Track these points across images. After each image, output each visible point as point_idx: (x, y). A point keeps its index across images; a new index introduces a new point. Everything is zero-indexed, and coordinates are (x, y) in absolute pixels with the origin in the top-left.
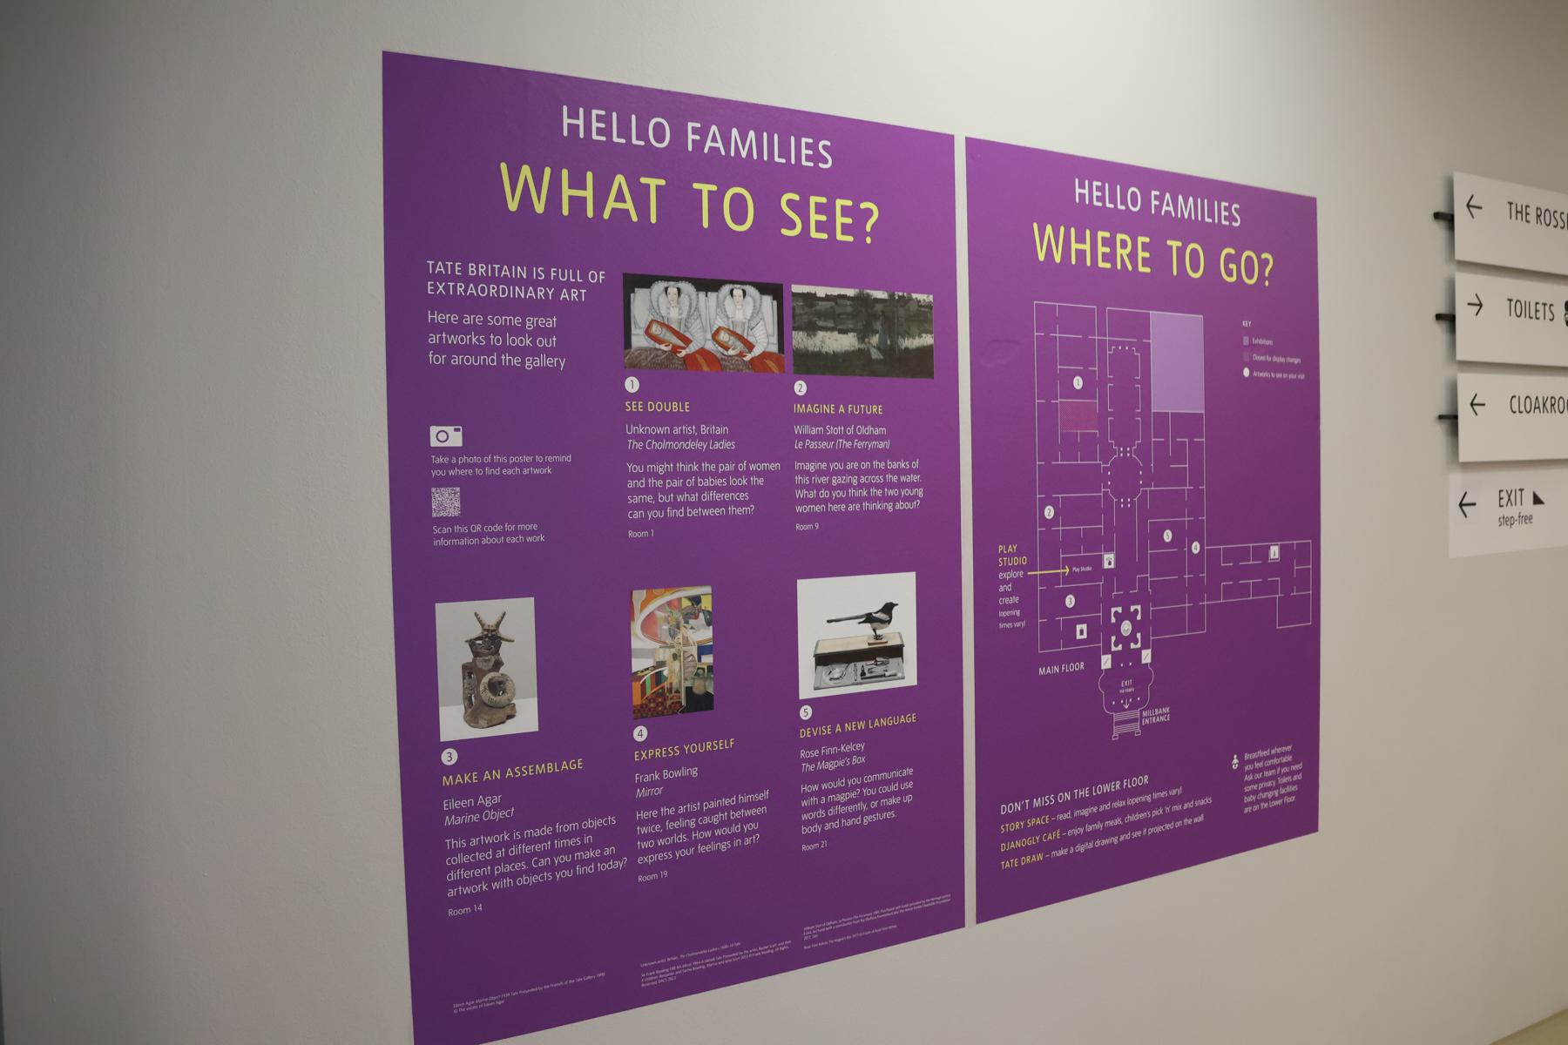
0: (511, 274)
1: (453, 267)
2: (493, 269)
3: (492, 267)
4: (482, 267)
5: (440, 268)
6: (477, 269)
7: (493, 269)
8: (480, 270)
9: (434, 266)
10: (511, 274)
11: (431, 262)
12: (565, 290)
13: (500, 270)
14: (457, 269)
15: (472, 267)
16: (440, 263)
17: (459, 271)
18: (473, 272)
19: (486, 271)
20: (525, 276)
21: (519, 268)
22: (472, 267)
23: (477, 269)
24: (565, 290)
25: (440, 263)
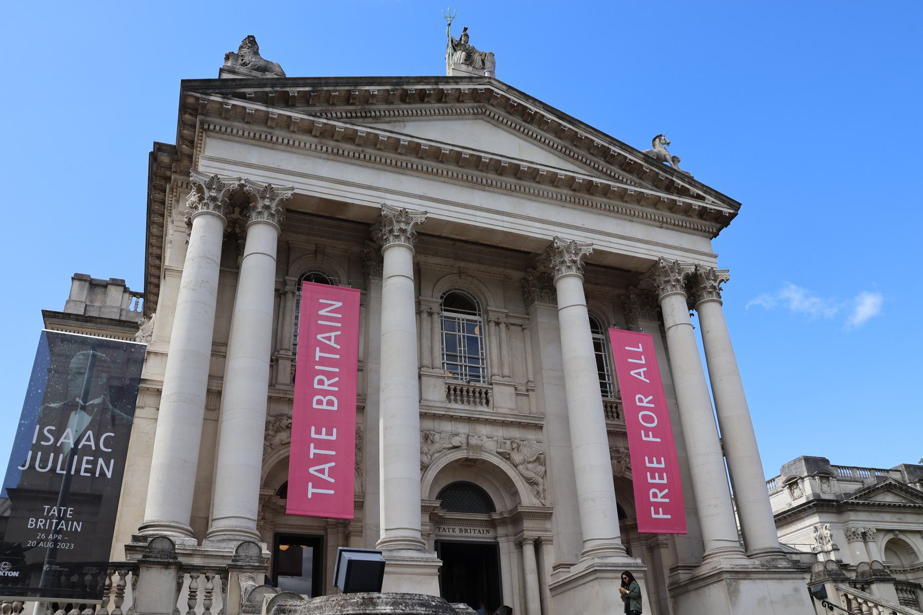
0: (336, 329)
1: (320, 444)
2: (323, 361)
3: (319, 363)
4: (321, 382)
5: (322, 471)
6: (325, 393)
7: (323, 361)
8: (325, 387)
9: (319, 483)
10: (336, 329)
11: (311, 490)
12: (632, 373)
13: (325, 348)
14: (323, 436)
15: (320, 402)
16: (312, 470)
17: (329, 433)
18: (330, 403)
19: (330, 375)
20: (339, 304)
21: (322, 312)
22: (320, 402)
23: (325, 393)
24: (632, 373)
25: (312, 470)
